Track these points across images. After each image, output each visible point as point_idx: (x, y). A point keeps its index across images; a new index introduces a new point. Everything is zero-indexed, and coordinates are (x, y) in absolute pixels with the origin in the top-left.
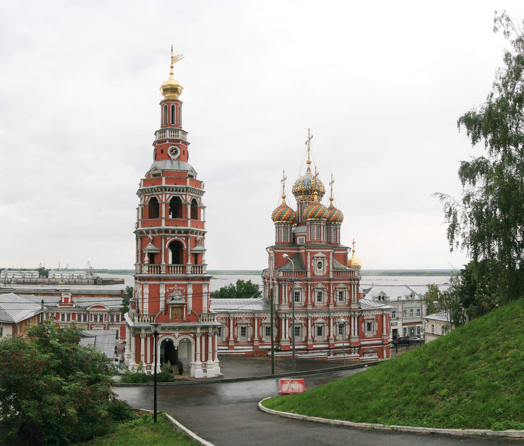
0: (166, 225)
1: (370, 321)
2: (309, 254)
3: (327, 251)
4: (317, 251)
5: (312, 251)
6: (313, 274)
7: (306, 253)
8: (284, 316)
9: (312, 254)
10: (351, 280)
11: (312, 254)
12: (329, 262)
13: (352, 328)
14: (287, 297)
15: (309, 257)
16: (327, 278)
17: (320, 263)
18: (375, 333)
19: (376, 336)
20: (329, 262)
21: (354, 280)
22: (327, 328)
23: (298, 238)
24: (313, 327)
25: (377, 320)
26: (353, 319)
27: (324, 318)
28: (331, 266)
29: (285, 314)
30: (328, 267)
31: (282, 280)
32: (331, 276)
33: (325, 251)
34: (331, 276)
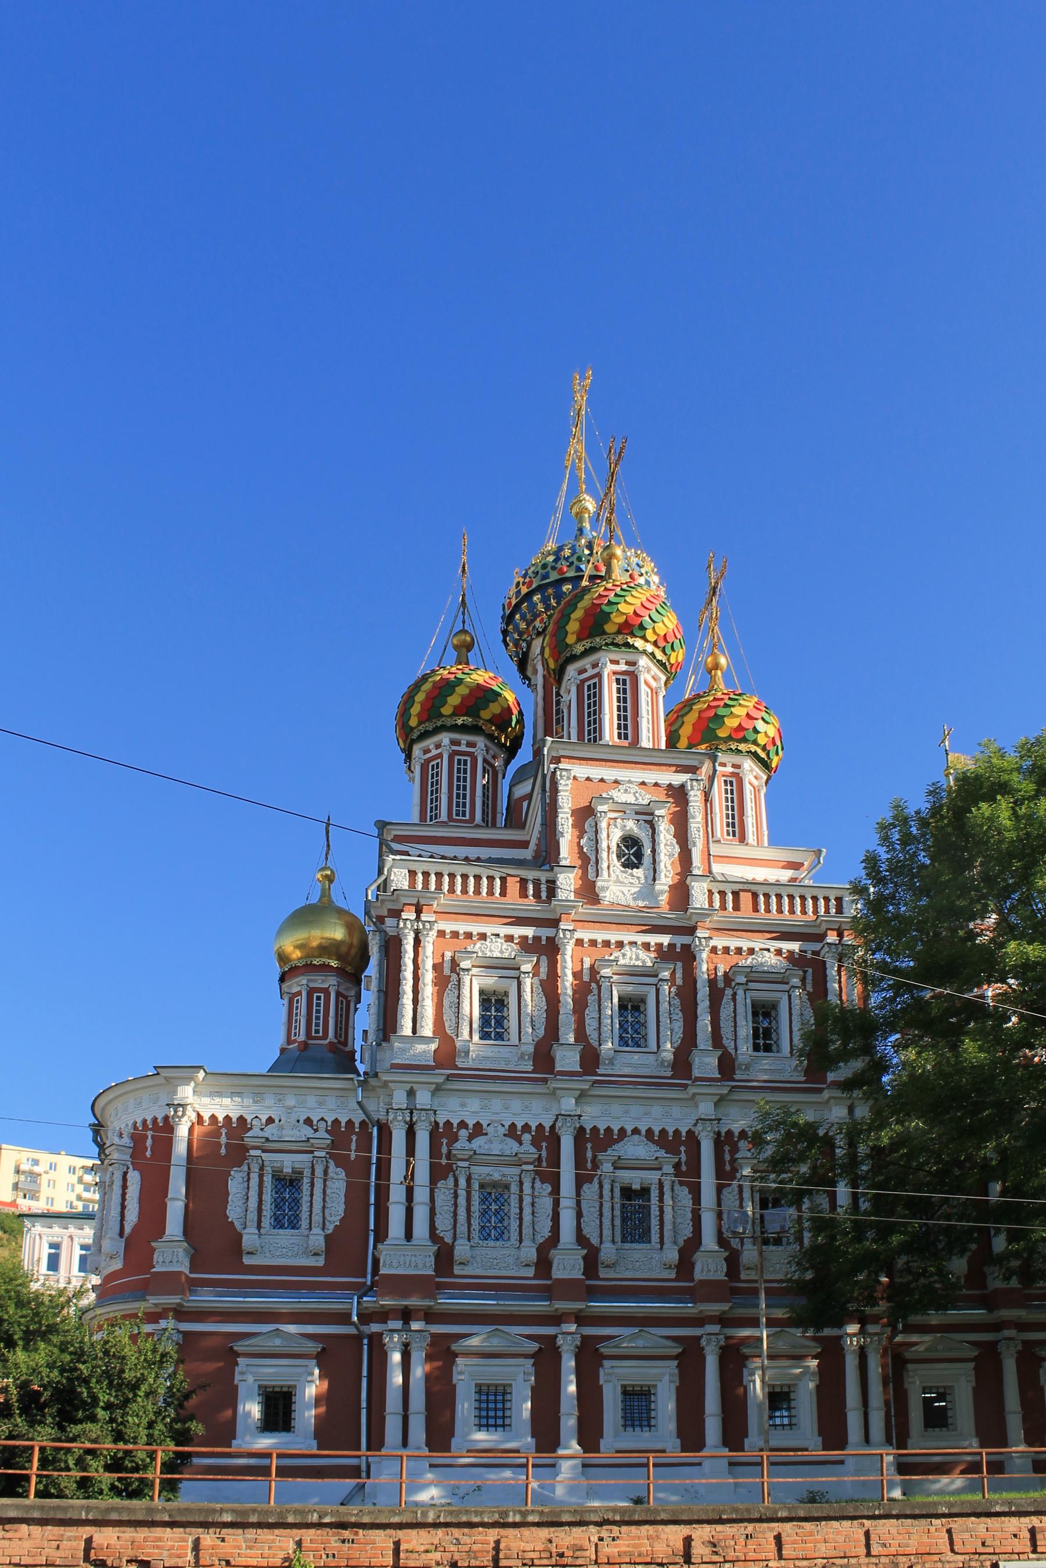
8: (400, 1099)
24: (590, 1190)
27: (664, 1140)
29: (411, 1093)
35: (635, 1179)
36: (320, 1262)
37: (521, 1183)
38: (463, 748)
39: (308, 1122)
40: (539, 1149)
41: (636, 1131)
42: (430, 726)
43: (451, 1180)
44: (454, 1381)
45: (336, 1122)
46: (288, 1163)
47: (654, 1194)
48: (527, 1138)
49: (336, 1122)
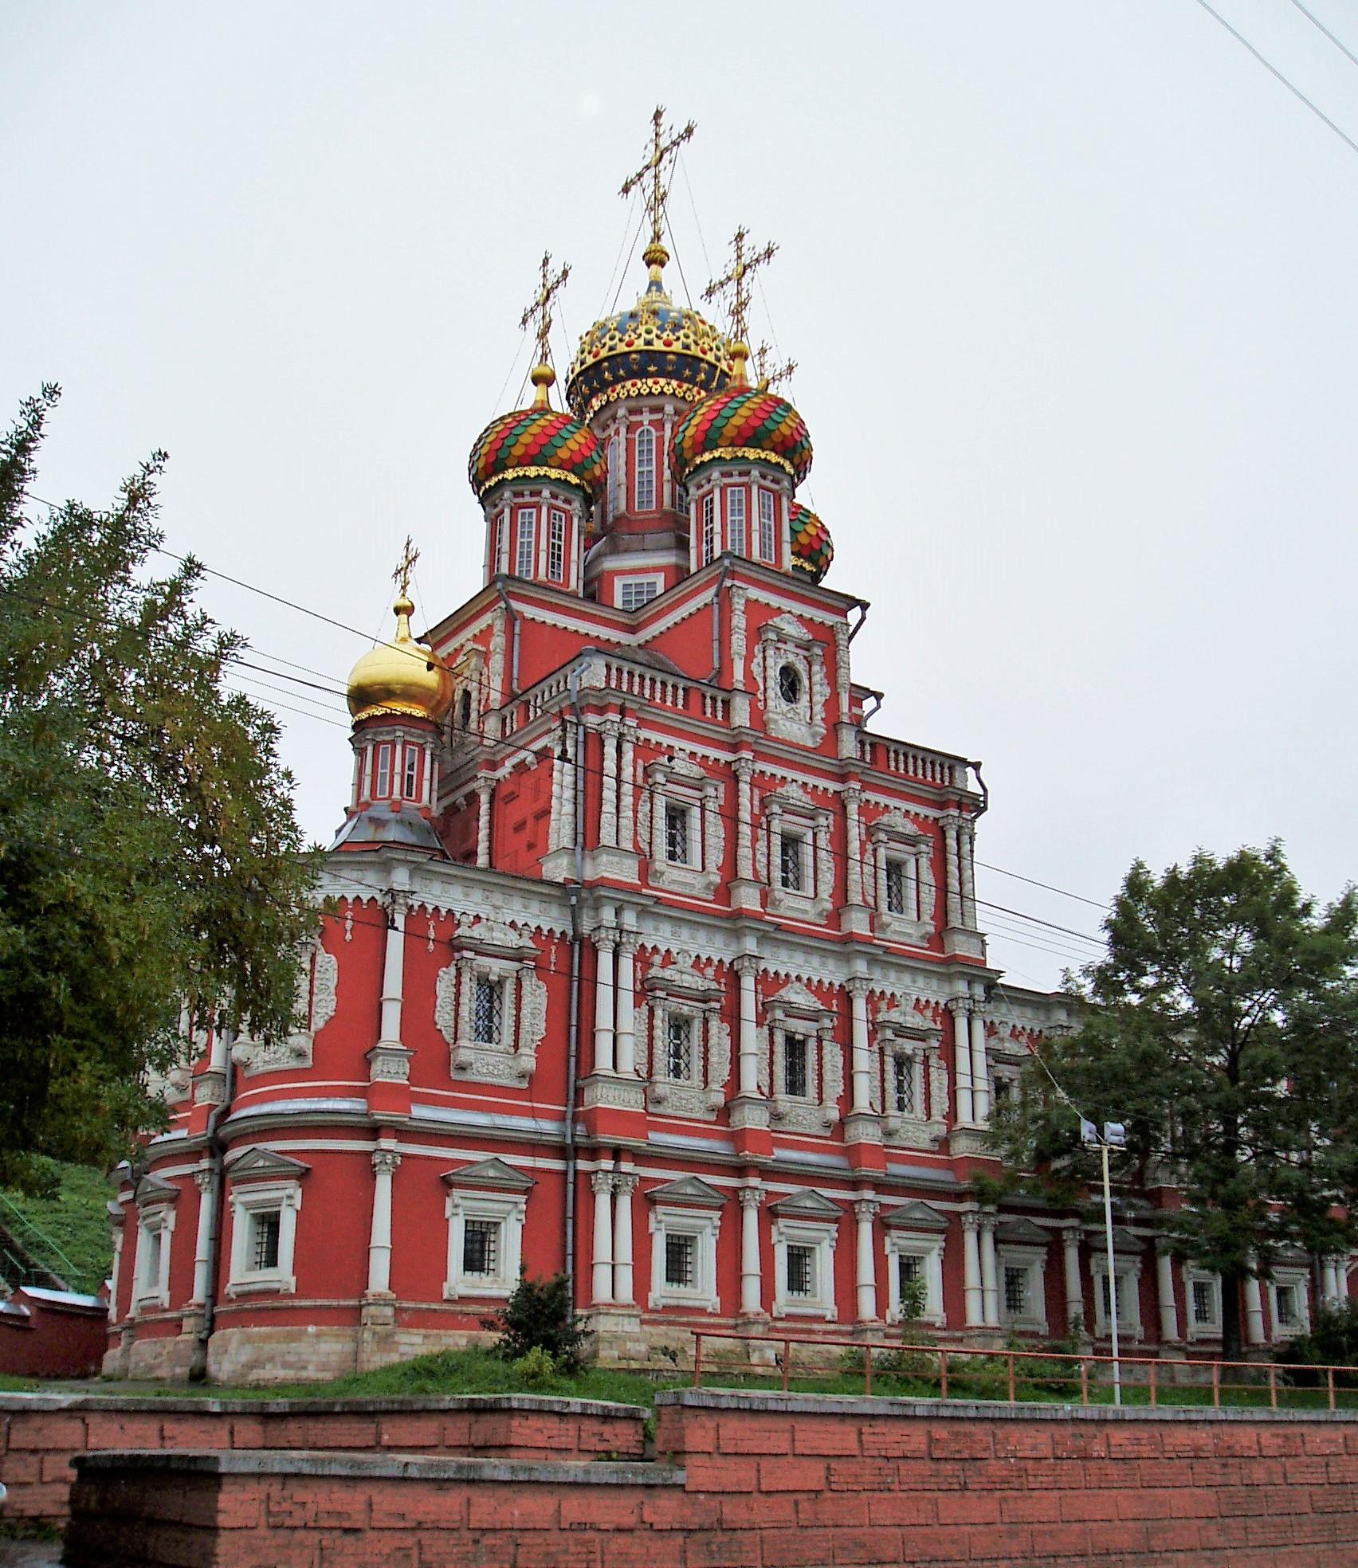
2: (739, 604)
4: (775, 601)
5: (754, 593)
6: (759, 719)
8: (608, 915)
10: (942, 805)
13: (963, 1081)
14: (628, 813)
15: (739, 621)
22: (833, 1054)
23: (618, 584)
26: (961, 1024)
31: (601, 711)
33: (819, 616)
35: (800, 1027)
36: (525, 1085)
37: (706, 1021)
38: (559, 503)
39: (513, 925)
40: (719, 983)
41: (798, 978)
42: (532, 471)
43: (645, 1008)
44: (651, 1230)
45: (538, 928)
46: (496, 968)
47: (812, 1045)
48: (710, 972)
49: (538, 928)
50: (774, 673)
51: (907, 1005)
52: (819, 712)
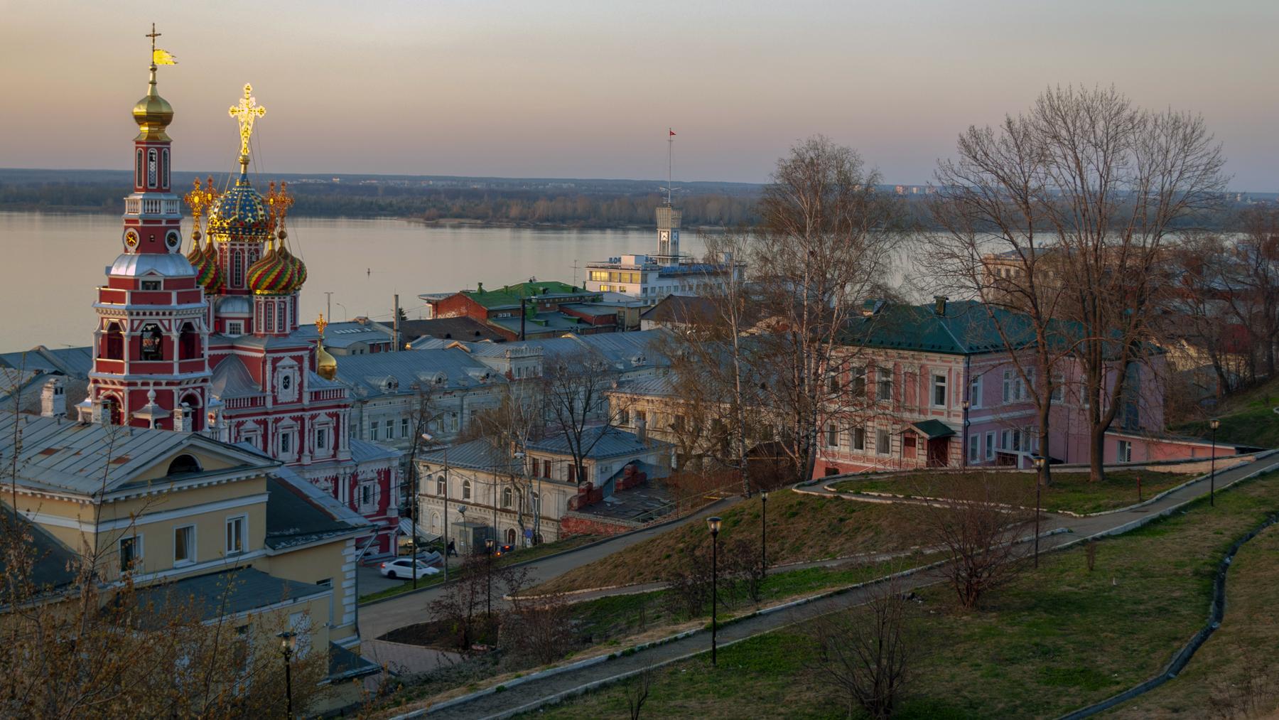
0: (181, 371)
1: (367, 484)
3: (299, 353)
7: (265, 362)
9: (275, 361)
10: (339, 406)
11: (275, 361)
12: (301, 375)
15: (269, 367)
16: (298, 406)
17: (286, 378)
18: (377, 507)
19: (379, 513)
20: (301, 375)
21: (345, 406)
23: (228, 322)
25: (380, 482)
28: (306, 384)
30: (301, 385)
32: (306, 401)
34: (306, 401)
50: (281, 380)
51: (322, 480)
52: (297, 388)
